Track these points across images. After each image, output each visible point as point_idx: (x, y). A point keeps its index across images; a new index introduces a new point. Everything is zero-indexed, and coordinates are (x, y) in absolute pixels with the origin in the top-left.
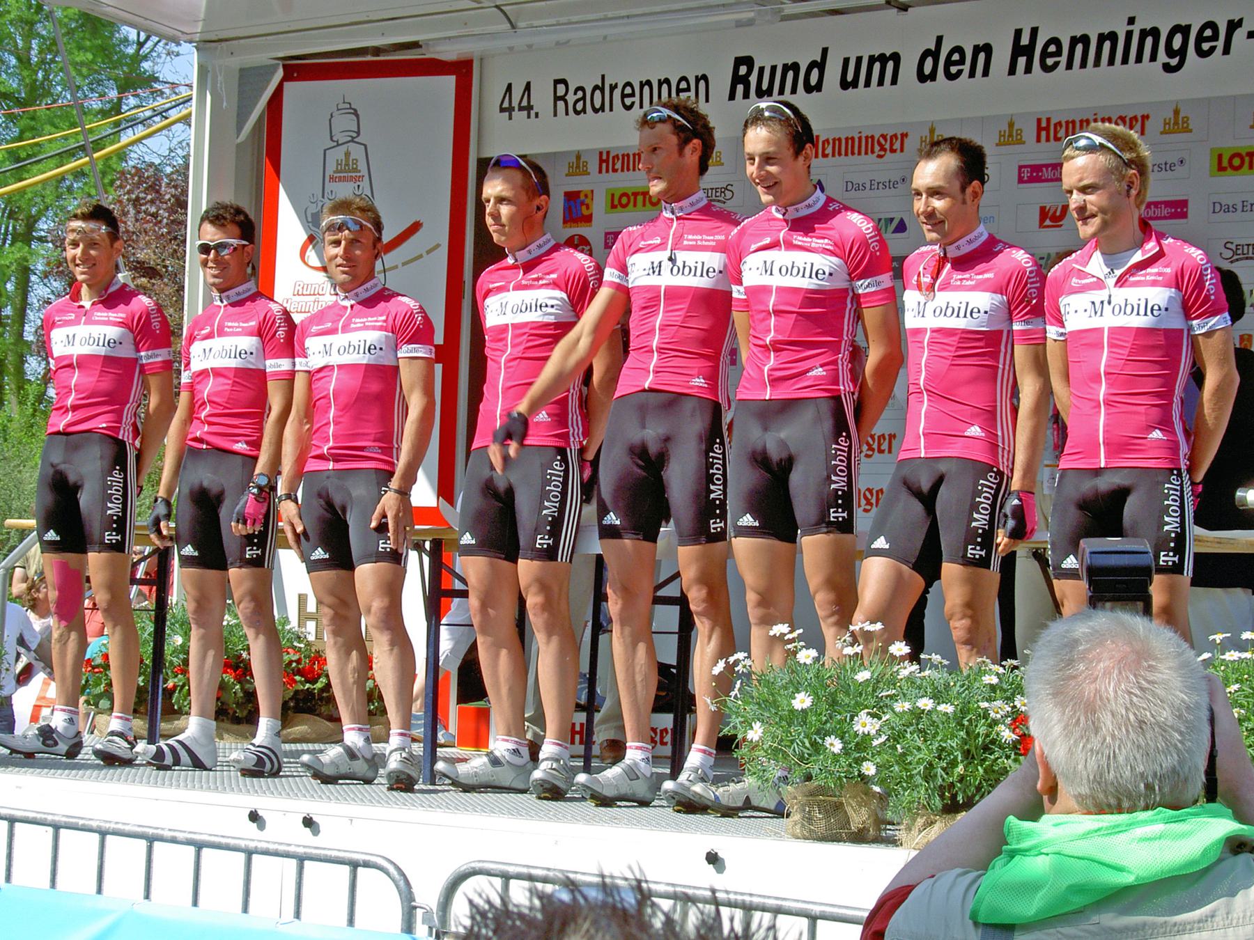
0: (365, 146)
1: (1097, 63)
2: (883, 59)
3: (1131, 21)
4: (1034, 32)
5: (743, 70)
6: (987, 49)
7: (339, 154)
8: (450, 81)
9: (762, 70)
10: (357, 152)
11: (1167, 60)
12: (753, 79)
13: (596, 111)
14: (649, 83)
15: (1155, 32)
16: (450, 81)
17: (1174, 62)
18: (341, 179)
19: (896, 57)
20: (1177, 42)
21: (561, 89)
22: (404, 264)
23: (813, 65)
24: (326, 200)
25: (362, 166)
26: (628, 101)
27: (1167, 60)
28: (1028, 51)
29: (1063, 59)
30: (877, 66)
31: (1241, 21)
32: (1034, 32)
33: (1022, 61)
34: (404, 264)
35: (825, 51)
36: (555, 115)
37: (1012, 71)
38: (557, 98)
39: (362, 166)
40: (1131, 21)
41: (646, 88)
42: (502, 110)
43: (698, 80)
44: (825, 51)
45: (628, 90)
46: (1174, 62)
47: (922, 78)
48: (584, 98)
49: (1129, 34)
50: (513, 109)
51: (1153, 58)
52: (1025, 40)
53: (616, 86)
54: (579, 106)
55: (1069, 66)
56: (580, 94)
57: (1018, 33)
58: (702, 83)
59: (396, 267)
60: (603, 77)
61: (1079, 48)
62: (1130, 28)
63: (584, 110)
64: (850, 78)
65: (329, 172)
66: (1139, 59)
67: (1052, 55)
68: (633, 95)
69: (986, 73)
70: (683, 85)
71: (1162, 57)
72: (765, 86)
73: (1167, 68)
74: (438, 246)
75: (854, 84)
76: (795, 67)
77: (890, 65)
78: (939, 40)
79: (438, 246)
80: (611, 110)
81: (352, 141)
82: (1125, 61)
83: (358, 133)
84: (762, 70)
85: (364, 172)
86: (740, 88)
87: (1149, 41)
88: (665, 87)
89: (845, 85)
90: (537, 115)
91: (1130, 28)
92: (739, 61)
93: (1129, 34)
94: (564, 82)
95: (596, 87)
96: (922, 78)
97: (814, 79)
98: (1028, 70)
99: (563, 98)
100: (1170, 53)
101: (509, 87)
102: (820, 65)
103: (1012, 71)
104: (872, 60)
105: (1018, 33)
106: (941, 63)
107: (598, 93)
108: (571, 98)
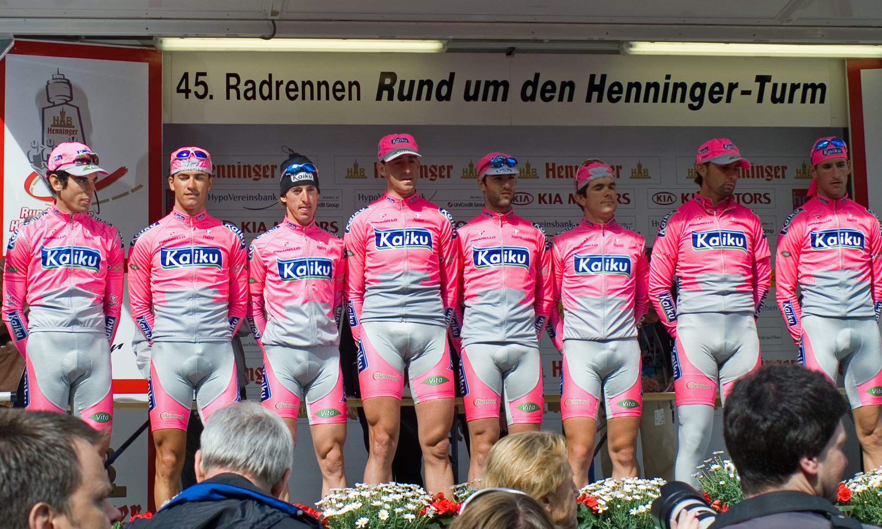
0: (78, 108)
2: (496, 84)
3: (668, 77)
5: (388, 81)
6: (571, 85)
7: (56, 112)
8: (143, 68)
9: (403, 83)
10: (70, 112)
12: (396, 88)
13: (264, 98)
14: (310, 83)
15: (683, 85)
16: (143, 68)
17: (696, 104)
19: (506, 84)
20: (698, 92)
21: (233, 81)
22: (114, 198)
23: (442, 83)
24: (45, 146)
26: (292, 94)
28: (600, 88)
29: (624, 96)
30: (492, 88)
32: (604, 77)
33: (595, 95)
34: (114, 198)
35: (452, 75)
36: (228, 98)
37: (589, 100)
38: (229, 87)
40: (668, 77)
41: (308, 87)
42: (179, 91)
44: (452, 75)
45: (292, 86)
46: (696, 104)
47: (524, 98)
48: (254, 88)
49: (667, 85)
52: (597, 82)
53: (282, 82)
54: (250, 94)
56: (250, 86)
57: (593, 77)
58: (354, 88)
59: (108, 200)
60: (270, 75)
62: (667, 81)
63: (254, 97)
64: (472, 93)
66: (673, 100)
67: (616, 92)
68: (296, 90)
69: (570, 99)
70: (339, 87)
71: (688, 100)
72: (405, 93)
73: (691, 107)
75: (475, 97)
76: (429, 83)
77: (501, 89)
78: (537, 76)
80: (278, 98)
81: (66, 103)
82: (664, 100)
83: (71, 98)
84: (403, 83)
86: (385, 93)
87: (680, 90)
88: (323, 87)
89: (467, 98)
90: (211, 97)
91: (667, 81)
92: (384, 75)
93: (667, 85)
94: (236, 76)
95: (264, 82)
96: (524, 98)
97: (444, 91)
98: (600, 100)
99: (235, 87)
100: (693, 98)
101: (186, 76)
102: (450, 83)
103: (589, 100)
104: (488, 84)
105: (593, 77)
106: (537, 90)
107: (266, 87)
108: (242, 88)
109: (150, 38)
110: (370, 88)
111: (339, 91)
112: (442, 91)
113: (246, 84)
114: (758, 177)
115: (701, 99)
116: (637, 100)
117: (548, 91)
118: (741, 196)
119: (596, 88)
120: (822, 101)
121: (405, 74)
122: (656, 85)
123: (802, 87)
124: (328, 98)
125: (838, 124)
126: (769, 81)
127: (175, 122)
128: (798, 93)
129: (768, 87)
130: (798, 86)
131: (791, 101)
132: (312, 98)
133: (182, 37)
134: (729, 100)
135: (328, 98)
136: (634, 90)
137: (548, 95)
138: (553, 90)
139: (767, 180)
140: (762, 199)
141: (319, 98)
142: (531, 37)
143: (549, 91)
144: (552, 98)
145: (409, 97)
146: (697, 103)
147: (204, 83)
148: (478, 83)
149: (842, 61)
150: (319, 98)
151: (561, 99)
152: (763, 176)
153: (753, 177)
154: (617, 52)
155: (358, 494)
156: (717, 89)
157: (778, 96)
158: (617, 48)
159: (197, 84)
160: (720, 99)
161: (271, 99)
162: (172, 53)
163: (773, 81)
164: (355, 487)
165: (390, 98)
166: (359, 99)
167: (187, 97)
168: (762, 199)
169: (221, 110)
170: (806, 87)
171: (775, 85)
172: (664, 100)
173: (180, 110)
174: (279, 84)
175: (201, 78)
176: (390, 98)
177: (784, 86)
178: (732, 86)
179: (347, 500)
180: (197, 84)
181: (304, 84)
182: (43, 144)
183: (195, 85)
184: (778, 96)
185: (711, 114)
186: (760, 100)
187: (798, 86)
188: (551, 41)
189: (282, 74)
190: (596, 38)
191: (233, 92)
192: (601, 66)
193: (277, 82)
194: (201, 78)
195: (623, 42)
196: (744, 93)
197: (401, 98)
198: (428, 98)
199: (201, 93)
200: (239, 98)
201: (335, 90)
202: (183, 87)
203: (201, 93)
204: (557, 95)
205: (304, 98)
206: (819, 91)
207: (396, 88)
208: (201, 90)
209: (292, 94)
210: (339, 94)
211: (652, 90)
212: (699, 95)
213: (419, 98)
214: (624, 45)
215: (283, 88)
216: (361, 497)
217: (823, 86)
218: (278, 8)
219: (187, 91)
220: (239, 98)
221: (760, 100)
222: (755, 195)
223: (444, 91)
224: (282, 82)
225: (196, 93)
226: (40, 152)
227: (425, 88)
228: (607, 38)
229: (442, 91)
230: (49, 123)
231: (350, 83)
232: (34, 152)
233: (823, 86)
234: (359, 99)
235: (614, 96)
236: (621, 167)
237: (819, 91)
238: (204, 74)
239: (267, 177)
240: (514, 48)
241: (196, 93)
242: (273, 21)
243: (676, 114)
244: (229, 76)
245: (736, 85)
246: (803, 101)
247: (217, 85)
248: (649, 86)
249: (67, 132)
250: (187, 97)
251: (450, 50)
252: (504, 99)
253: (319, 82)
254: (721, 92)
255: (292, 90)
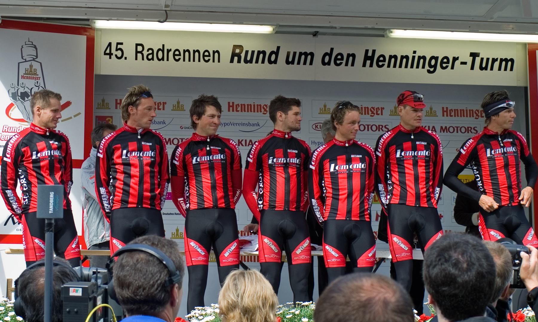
0: (41, 63)
1: (400, 66)
2: (306, 54)
3: (415, 52)
4: (374, 51)
5: (237, 51)
6: (354, 56)
7: (27, 65)
8: (82, 40)
9: (247, 52)
10: (36, 66)
11: (429, 69)
12: (243, 55)
13: (159, 60)
14: (188, 51)
15: (424, 58)
16: (82, 40)
17: (432, 70)
18: (30, 78)
19: (312, 54)
23: (272, 53)
24: (19, 87)
25: (39, 72)
26: (177, 58)
27: (429, 69)
28: (371, 58)
31: (458, 57)
32: (374, 51)
33: (368, 62)
35: (278, 48)
36: (136, 59)
37: (364, 65)
38: (137, 52)
39: (39, 72)
40: (415, 52)
41: (187, 53)
42: (105, 54)
43: (214, 52)
44: (278, 48)
45: (177, 53)
46: (432, 70)
47: (324, 63)
48: (153, 53)
49: (414, 57)
50: (112, 54)
51: (423, 67)
52: (370, 54)
53: (171, 50)
54: (150, 57)
55: (389, 66)
56: (150, 52)
57: (367, 51)
58: (216, 54)
60: (163, 45)
61: (393, 60)
62: (414, 55)
63: (153, 59)
64: (290, 60)
65: (22, 73)
66: (418, 67)
68: (180, 55)
69: (353, 65)
70: (207, 54)
72: (249, 58)
73: (429, 71)
74: (79, 114)
75: (292, 62)
76: (264, 53)
77: (309, 57)
78: (332, 50)
79: (79, 114)
80: (168, 60)
81: (34, 60)
82: (412, 67)
83: (37, 57)
84: (247, 52)
85: (40, 75)
86: (236, 59)
87: (422, 61)
88: (197, 54)
89: (288, 62)
90: (126, 58)
91: (414, 55)
93: (414, 57)
95: (159, 50)
96: (324, 63)
97: (273, 57)
98: (371, 65)
99: (141, 52)
101: (110, 45)
102: (277, 53)
103: (364, 65)
104: (301, 54)
105: (367, 51)
106: (331, 58)
107: (160, 53)
108: (145, 53)
109: (88, 20)
110: (226, 55)
111: (206, 56)
112: (272, 58)
113: (148, 51)
114: (470, 116)
115: (435, 66)
116: (395, 66)
117: (339, 60)
118: (459, 128)
119: (369, 58)
120: (511, 69)
121: (249, 46)
122: (407, 57)
123: (499, 60)
124: (199, 61)
125: (521, 84)
126: (478, 56)
127: (103, 73)
128: (497, 64)
129: (478, 60)
130: (497, 60)
131: (492, 69)
132: (189, 61)
133: (108, 20)
134: (452, 68)
135: (199, 61)
136: (393, 60)
137: (338, 62)
138: (342, 59)
139: (476, 118)
140: (473, 130)
141: (194, 61)
142: (328, 25)
143: (339, 59)
144: (341, 63)
145: (251, 61)
146: (432, 70)
147: (121, 50)
148: (295, 53)
149: (525, 44)
150: (194, 61)
151: (347, 65)
152: (473, 116)
153: (467, 116)
154: (383, 36)
155: (212, 310)
156: (445, 60)
157: (484, 65)
158: (381, 33)
159: (117, 50)
160: (447, 67)
161: (163, 60)
162: (100, 30)
163: (481, 56)
164: (211, 306)
165: (239, 61)
166: (219, 61)
167: (110, 58)
168: (473, 130)
169: (131, 67)
170: (502, 60)
171: (482, 59)
172: (412, 67)
173: (106, 66)
174: (169, 51)
175: (119, 46)
176: (239, 61)
177: (488, 59)
178: (455, 59)
179: (206, 314)
180: (117, 50)
181: (185, 51)
182: (18, 85)
183: (114, 51)
184: (484, 65)
185: (442, 77)
186: (472, 68)
187: (497, 60)
188: (342, 28)
189: (171, 44)
190: (369, 27)
191: (139, 55)
192: (371, 44)
193: (168, 50)
194: (119, 46)
195: (387, 29)
196: (463, 63)
197: (246, 61)
198: (263, 62)
199: (119, 55)
200: (143, 59)
201: (204, 56)
202: (108, 51)
203: (119, 55)
204: (344, 62)
205: (184, 60)
206: (510, 63)
207: (243, 55)
208: (119, 53)
209: (177, 58)
210: (207, 58)
211: (405, 60)
212: (434, 64)
213: (257, 62)
214: (388, 32)
215: (171, 54)
216: (214, 312)
217: (512, 60)
218: (169, 3)
219: (110, 54)
220: (143, 59)
221: (472, 68)
222: (468, 128)
223: (273, 57)
224: (171, 50)
225: (116, 56)
226: (16, 90)
227: (261, 56)
228: (376, 27)
229: (272, 58)
230: (22, 73)
231: (214, 51)
232: (13, 91)
233: (512, 60)
234: (219, 61)
235: (381, 64)
236: (384, 108)
237: (510, 63)
238: (122, 44)
239: (160, 109)
240: (318, 32)
241: (116, 56)
242: (166, 11)
243: (418, 76)
244: (137, 45)
245: (458, 58)
246: (500, 69)
247: (129, 50)
248: (402, 57)
249: (33, 78)
250: (110, 58)
251: (277, 32)
252: (311, 63)
253: (194, 50)
254: (448, 62)
255: (177, 55)
